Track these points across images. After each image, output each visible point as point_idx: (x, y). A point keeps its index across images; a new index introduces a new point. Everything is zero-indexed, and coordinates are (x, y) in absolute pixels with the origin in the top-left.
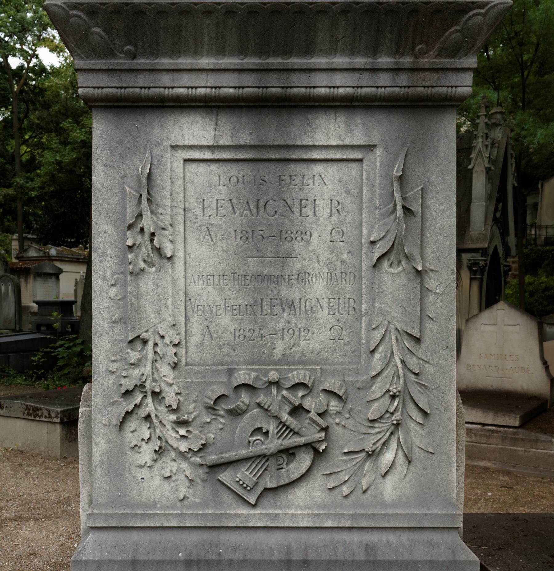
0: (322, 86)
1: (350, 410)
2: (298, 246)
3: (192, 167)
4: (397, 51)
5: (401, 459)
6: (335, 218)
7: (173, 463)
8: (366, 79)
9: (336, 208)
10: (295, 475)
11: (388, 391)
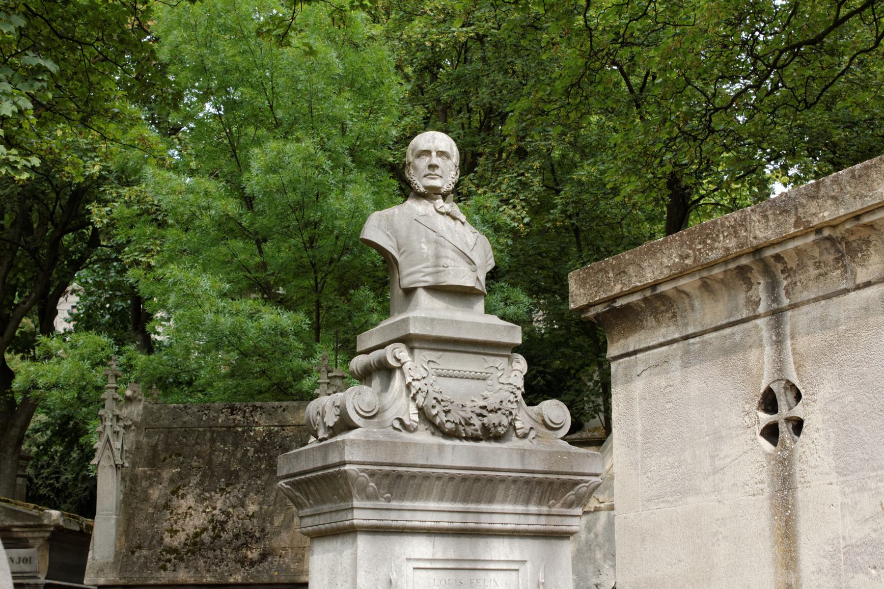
4: (540, 503)
8: (522, 519)
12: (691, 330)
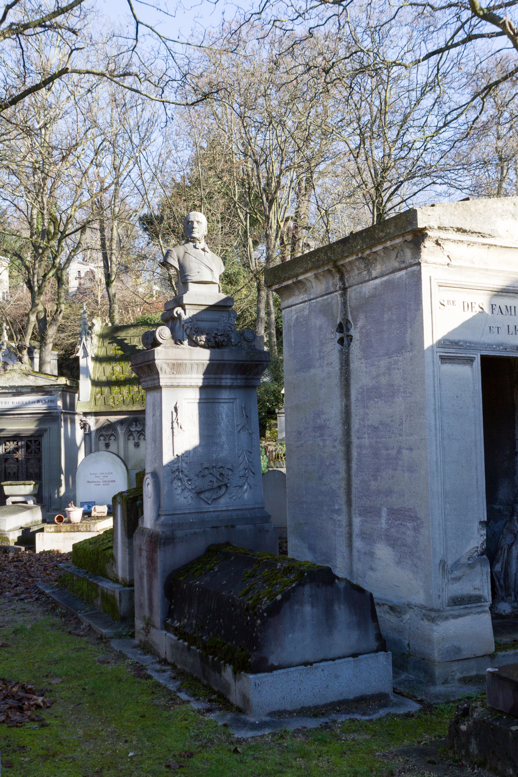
0: (224, 382)
2: (218, 427)
9: (227, 416)
12: (312, 297)
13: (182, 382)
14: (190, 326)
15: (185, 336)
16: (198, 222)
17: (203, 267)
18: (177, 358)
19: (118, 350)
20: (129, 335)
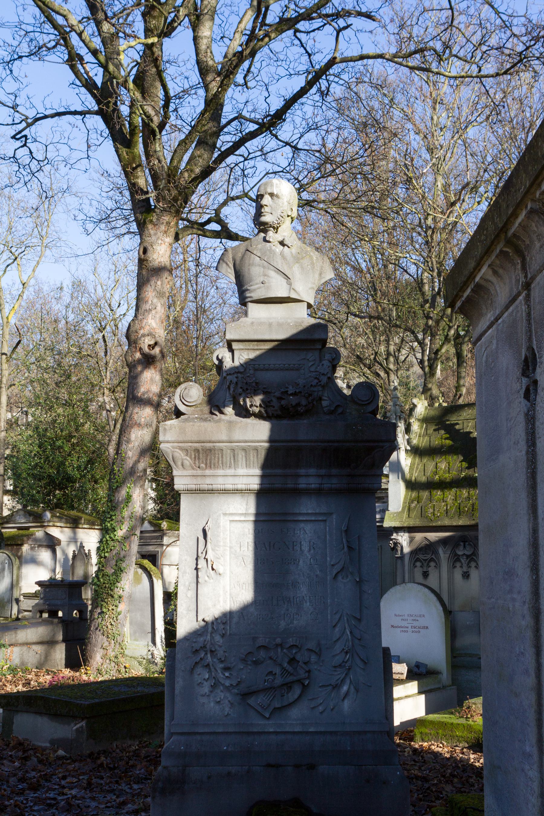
0: (303, 483)
1: (323, 661)
3: (233, 524)
5: (352, 689)
6: (312, 551)
7: (221, 693)
10: (291, 700)
11: (343, 649)
13: (219, 483)
14: (235, 380)
15: (229, 398)
16: (272, 195)
17: (272, 273)
18: (202, 438)
19: (446, 439)
20: (461, 418)
